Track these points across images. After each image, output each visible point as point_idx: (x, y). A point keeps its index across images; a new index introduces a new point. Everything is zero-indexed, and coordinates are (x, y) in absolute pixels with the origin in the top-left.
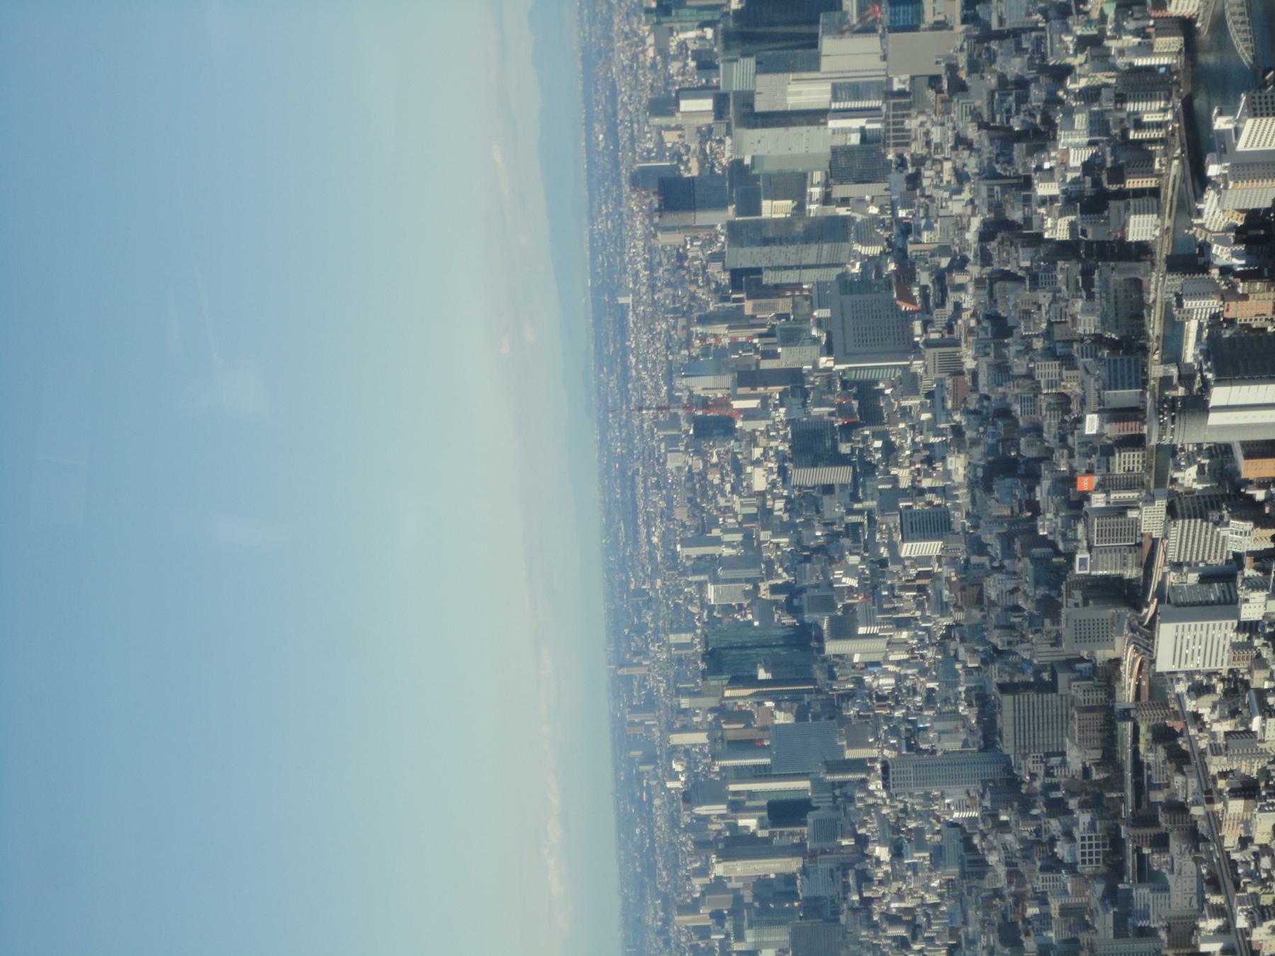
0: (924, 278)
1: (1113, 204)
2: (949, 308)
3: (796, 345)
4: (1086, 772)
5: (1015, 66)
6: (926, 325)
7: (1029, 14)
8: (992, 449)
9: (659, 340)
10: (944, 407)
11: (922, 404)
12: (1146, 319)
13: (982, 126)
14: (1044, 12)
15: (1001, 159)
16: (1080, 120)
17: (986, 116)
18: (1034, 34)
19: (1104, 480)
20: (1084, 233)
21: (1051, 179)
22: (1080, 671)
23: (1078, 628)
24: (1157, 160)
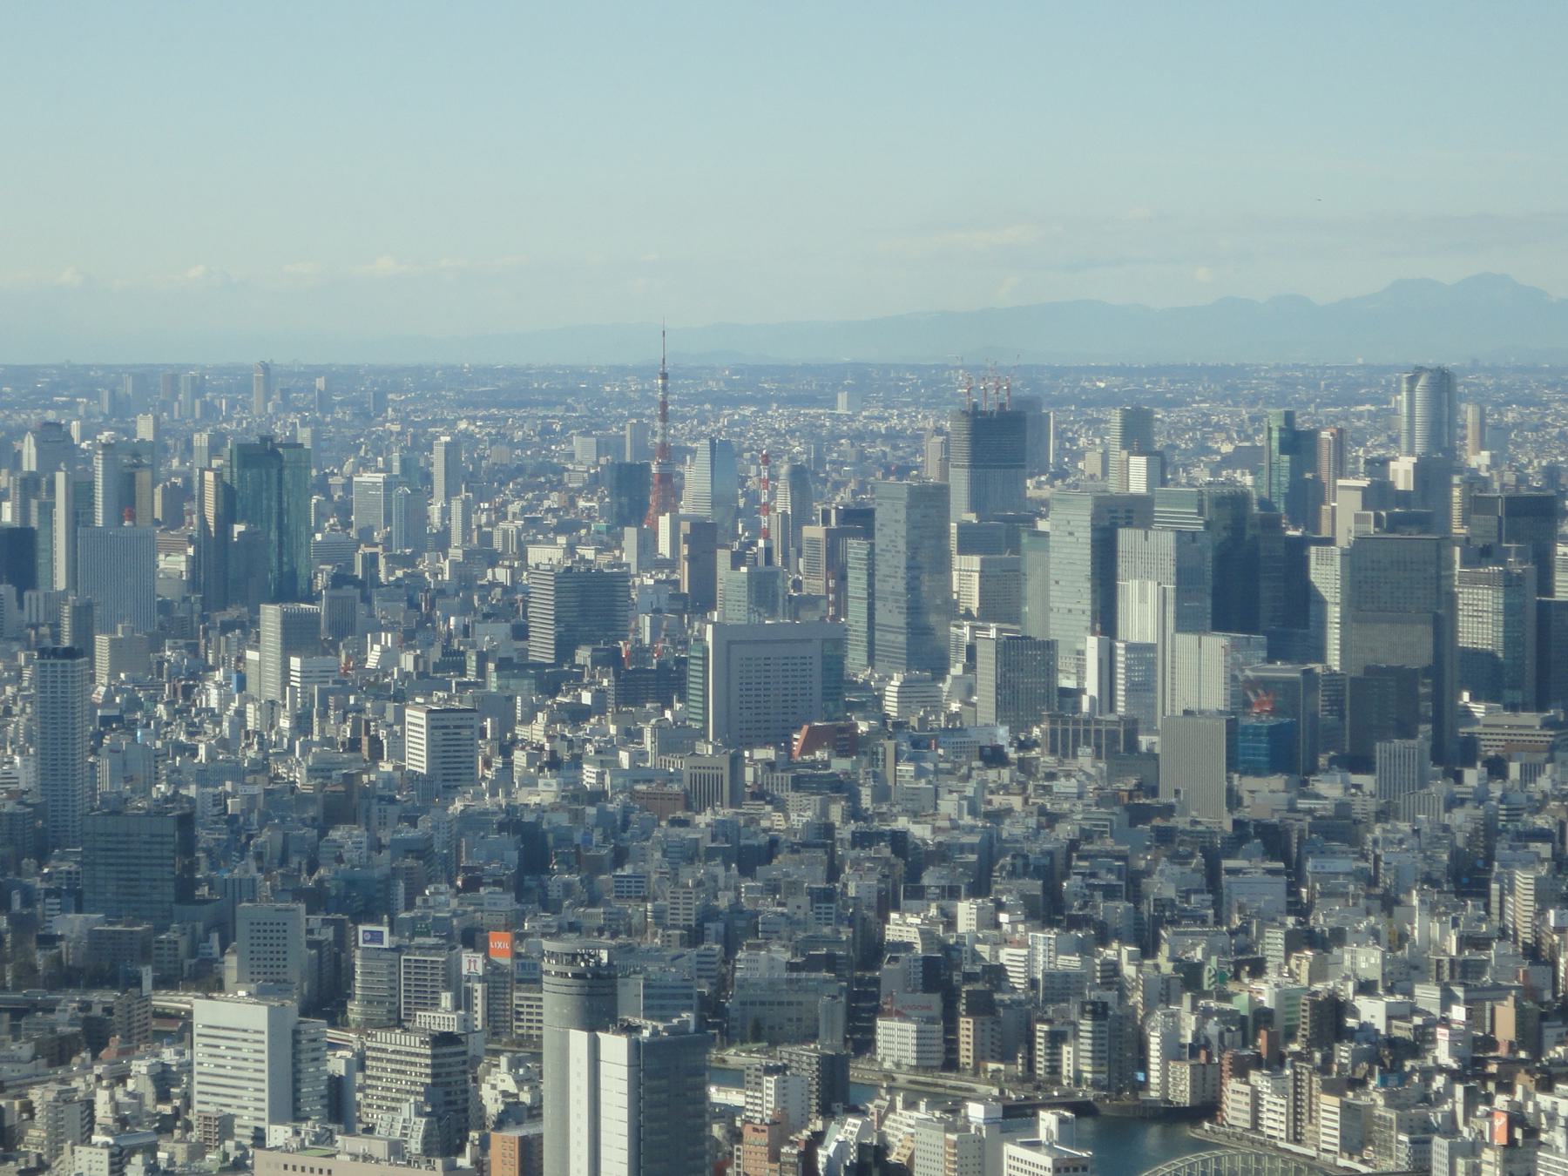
0: (840, 765)
1: (935, 1000)
2: (792, 797)
3: (750, 596)
4: (48, 941)
5: (1162, 884)
6: (770, 766)
7: (1241, 909)
8: (564, 838)
9: (776, 443)
10: (637, 782)
11: (643, 755)
12: (754, 1047)
13: (1073, 845)
14: (1244, 930)
15: (1019, 862)
16: (1071, 962)
17: (1085, 847)
18: (1211, 912)
19: (503, 974)
20: (896, 959)
21: (982, 924)
22: (207, 940)
23: (268, 927)
24: (1002, 1067)
